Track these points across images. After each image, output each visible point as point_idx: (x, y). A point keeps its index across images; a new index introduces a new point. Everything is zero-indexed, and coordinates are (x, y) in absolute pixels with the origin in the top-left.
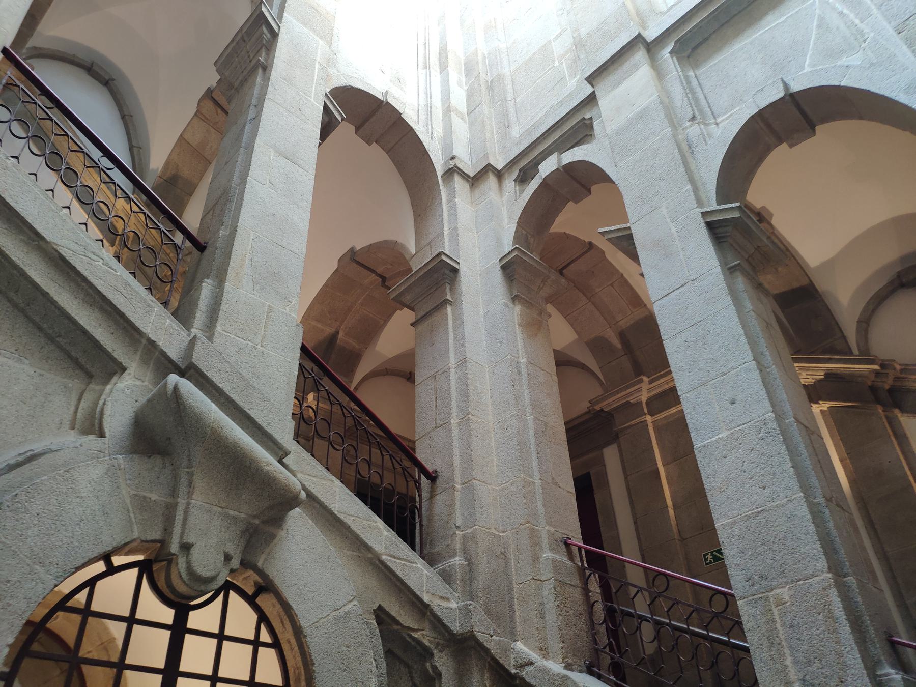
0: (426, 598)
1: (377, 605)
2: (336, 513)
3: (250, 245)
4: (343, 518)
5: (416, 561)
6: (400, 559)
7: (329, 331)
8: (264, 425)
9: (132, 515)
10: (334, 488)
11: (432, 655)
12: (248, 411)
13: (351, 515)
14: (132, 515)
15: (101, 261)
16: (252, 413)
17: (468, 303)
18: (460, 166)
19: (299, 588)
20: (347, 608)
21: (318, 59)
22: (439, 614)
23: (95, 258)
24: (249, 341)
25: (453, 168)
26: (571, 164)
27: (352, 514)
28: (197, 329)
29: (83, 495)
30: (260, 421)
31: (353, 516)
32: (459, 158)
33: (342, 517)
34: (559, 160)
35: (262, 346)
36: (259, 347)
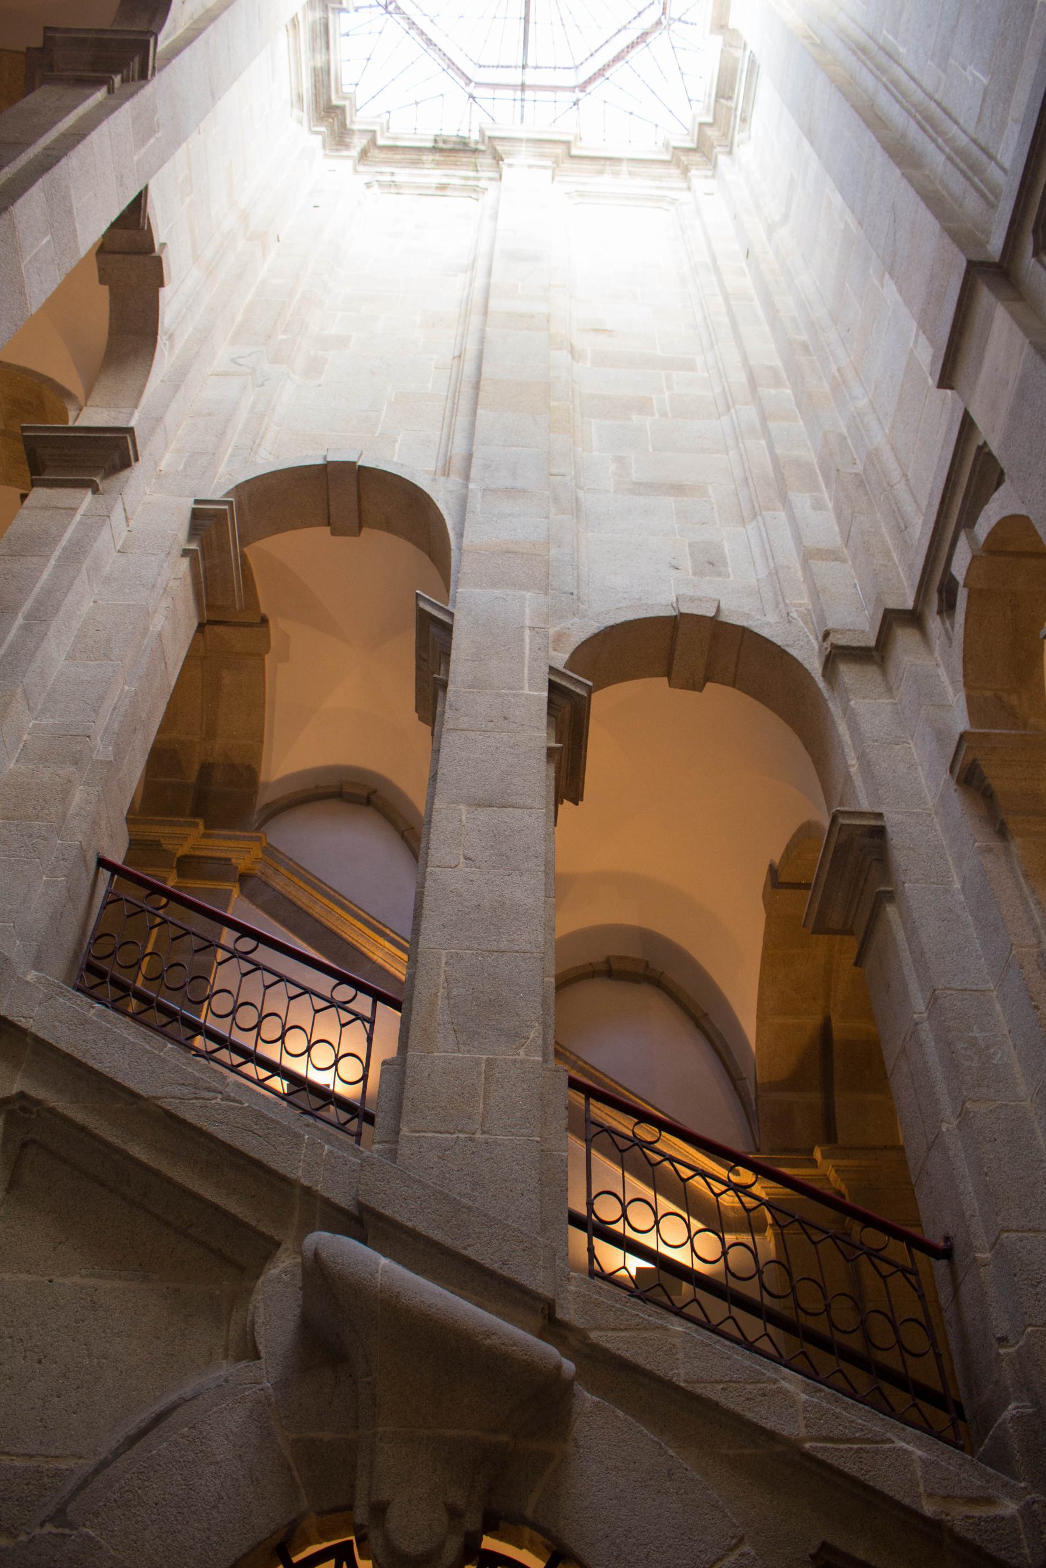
0: (929, 1509)
2: (683, 1384)
3: (442, 974)
4: (699, 1391)
5: (889, 1435)
6: (849, 1441)
7: (812, 1022)
9: (296, 1474)
10: (670, 1340)
12: (464, 1252)
13: (716, 1382)
14: (296, 1474)
15: (220, 1096)
16: (471, 1253)
17: (917, 881)
18: (843, 642)
19: (613, 1543)
21: (528, 623)
22: (970, 1536)
23: (211, 1094)
24: (460, 1132)
25: (830, 652)
26: (992, 534)
27: (718, 1377)
28: (379, 1143)
29: (219, 1458)
30: (487, 1263)
31: (720, 1382)
32: (836, 631)
33: (699, 1389)
34: (972, 539)
35: (483, 1132)
36: (478, 1135)
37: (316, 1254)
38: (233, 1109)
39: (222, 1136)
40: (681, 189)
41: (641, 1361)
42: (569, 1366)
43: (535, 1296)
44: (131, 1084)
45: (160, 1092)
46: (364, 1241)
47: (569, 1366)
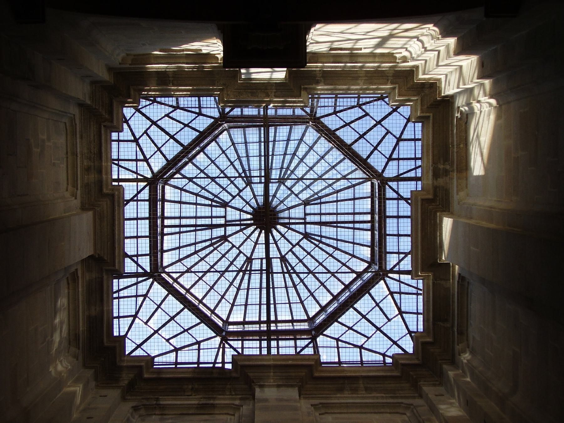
40: (414, 397)
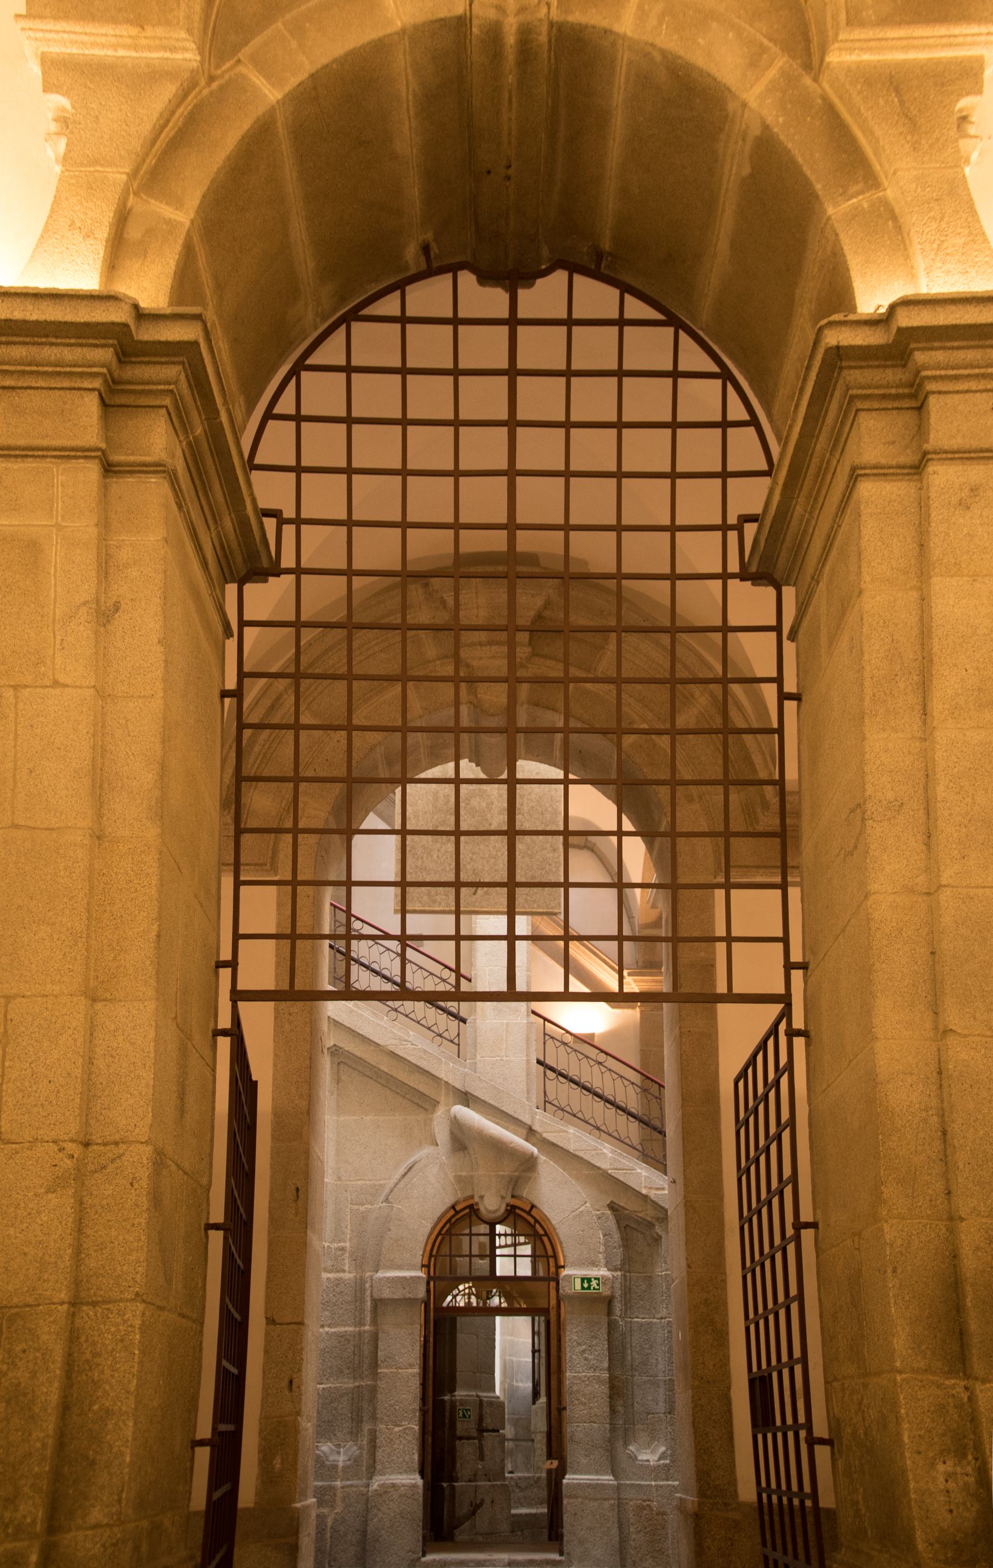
0: (644, 1191)
1: (609, 1201)
8: (512, 1114)
11: (654, 1225)
16: (504, 1109)
20: (581, 1210)
23: (406, 1043)
30: (509, 1112)
33: (577, 1153)
36: (504, 1058)
37: (455, 1117)
38: (415, 1049)
39: (413, 1061)
41: (559, 1144)
42: (535, 1150)
43: (525, 1124)
44: (376, 1040)
45: (388, 1043)
46: (468, 1106)
47: (535, 1150)
